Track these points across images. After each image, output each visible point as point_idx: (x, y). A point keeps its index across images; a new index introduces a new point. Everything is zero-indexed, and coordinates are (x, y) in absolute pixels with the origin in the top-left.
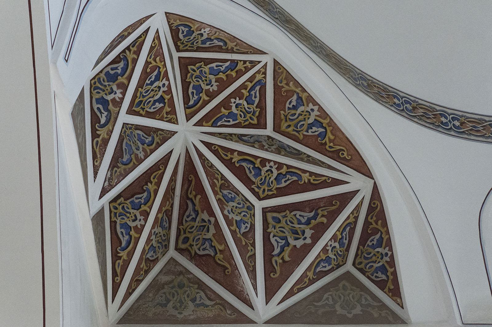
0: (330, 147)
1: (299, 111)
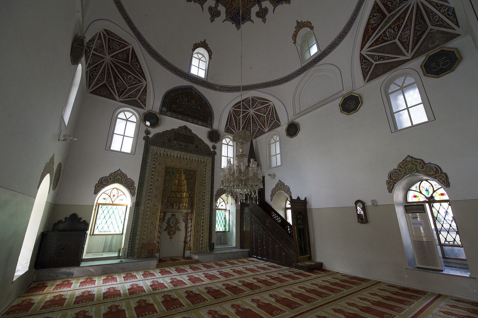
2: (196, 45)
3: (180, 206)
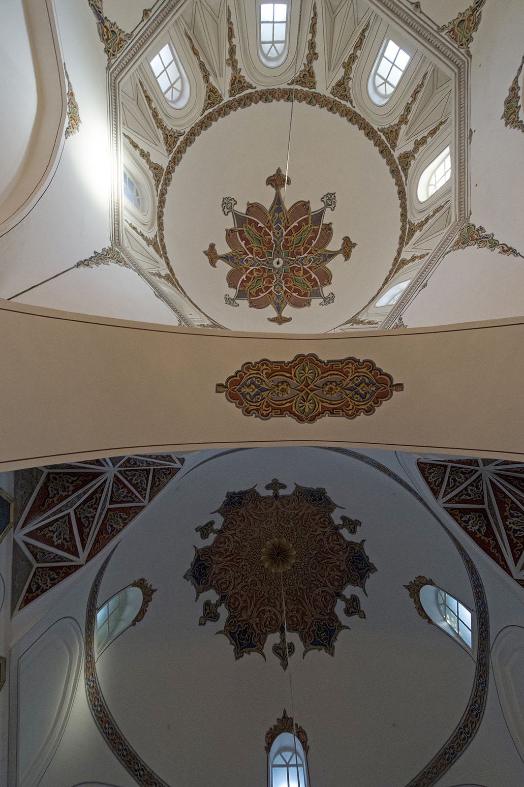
0: (101, 538)
1: (119, 519)
2: (270, 735)
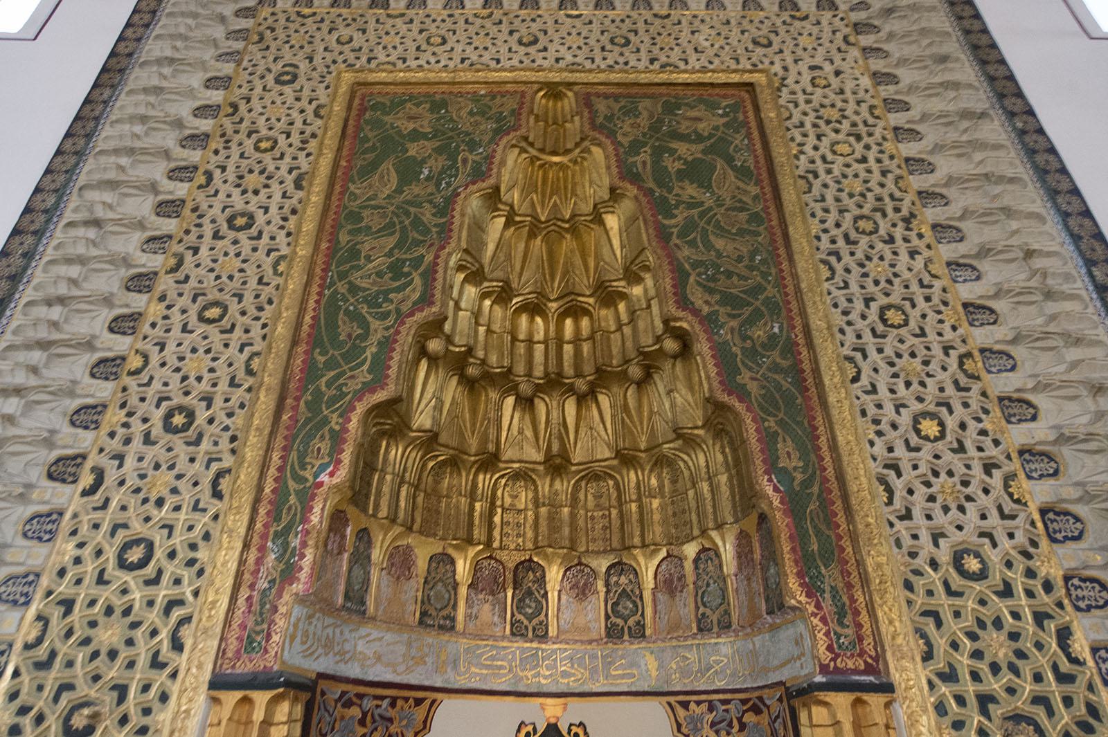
3: (632, 595)
